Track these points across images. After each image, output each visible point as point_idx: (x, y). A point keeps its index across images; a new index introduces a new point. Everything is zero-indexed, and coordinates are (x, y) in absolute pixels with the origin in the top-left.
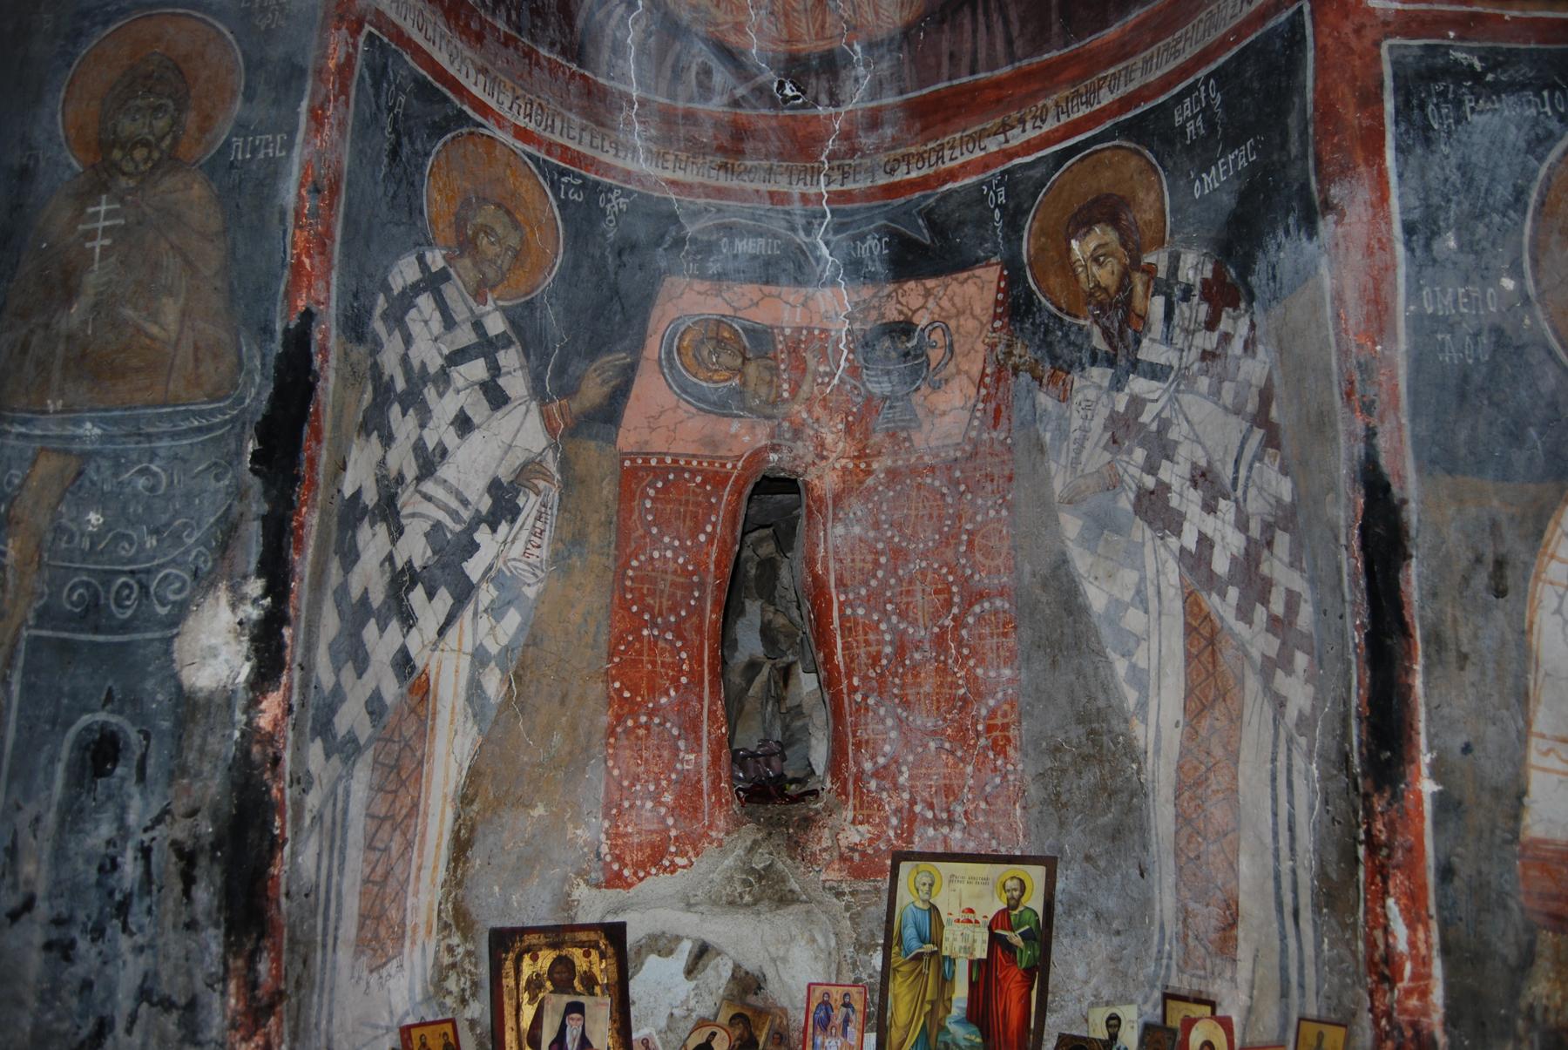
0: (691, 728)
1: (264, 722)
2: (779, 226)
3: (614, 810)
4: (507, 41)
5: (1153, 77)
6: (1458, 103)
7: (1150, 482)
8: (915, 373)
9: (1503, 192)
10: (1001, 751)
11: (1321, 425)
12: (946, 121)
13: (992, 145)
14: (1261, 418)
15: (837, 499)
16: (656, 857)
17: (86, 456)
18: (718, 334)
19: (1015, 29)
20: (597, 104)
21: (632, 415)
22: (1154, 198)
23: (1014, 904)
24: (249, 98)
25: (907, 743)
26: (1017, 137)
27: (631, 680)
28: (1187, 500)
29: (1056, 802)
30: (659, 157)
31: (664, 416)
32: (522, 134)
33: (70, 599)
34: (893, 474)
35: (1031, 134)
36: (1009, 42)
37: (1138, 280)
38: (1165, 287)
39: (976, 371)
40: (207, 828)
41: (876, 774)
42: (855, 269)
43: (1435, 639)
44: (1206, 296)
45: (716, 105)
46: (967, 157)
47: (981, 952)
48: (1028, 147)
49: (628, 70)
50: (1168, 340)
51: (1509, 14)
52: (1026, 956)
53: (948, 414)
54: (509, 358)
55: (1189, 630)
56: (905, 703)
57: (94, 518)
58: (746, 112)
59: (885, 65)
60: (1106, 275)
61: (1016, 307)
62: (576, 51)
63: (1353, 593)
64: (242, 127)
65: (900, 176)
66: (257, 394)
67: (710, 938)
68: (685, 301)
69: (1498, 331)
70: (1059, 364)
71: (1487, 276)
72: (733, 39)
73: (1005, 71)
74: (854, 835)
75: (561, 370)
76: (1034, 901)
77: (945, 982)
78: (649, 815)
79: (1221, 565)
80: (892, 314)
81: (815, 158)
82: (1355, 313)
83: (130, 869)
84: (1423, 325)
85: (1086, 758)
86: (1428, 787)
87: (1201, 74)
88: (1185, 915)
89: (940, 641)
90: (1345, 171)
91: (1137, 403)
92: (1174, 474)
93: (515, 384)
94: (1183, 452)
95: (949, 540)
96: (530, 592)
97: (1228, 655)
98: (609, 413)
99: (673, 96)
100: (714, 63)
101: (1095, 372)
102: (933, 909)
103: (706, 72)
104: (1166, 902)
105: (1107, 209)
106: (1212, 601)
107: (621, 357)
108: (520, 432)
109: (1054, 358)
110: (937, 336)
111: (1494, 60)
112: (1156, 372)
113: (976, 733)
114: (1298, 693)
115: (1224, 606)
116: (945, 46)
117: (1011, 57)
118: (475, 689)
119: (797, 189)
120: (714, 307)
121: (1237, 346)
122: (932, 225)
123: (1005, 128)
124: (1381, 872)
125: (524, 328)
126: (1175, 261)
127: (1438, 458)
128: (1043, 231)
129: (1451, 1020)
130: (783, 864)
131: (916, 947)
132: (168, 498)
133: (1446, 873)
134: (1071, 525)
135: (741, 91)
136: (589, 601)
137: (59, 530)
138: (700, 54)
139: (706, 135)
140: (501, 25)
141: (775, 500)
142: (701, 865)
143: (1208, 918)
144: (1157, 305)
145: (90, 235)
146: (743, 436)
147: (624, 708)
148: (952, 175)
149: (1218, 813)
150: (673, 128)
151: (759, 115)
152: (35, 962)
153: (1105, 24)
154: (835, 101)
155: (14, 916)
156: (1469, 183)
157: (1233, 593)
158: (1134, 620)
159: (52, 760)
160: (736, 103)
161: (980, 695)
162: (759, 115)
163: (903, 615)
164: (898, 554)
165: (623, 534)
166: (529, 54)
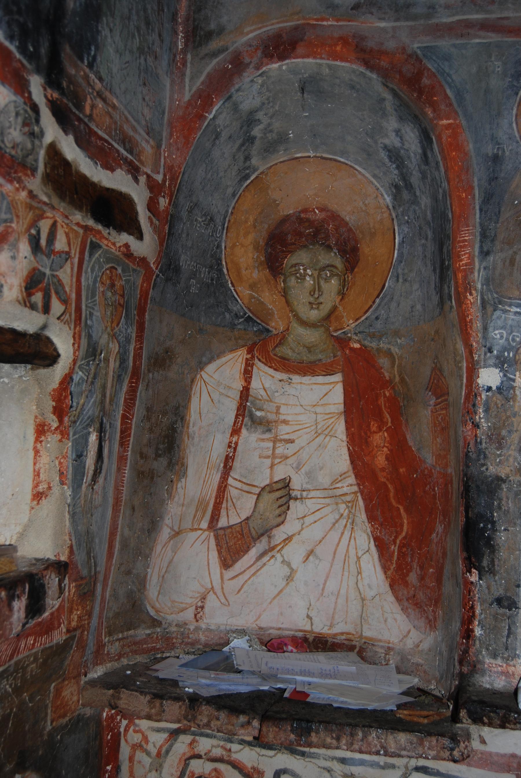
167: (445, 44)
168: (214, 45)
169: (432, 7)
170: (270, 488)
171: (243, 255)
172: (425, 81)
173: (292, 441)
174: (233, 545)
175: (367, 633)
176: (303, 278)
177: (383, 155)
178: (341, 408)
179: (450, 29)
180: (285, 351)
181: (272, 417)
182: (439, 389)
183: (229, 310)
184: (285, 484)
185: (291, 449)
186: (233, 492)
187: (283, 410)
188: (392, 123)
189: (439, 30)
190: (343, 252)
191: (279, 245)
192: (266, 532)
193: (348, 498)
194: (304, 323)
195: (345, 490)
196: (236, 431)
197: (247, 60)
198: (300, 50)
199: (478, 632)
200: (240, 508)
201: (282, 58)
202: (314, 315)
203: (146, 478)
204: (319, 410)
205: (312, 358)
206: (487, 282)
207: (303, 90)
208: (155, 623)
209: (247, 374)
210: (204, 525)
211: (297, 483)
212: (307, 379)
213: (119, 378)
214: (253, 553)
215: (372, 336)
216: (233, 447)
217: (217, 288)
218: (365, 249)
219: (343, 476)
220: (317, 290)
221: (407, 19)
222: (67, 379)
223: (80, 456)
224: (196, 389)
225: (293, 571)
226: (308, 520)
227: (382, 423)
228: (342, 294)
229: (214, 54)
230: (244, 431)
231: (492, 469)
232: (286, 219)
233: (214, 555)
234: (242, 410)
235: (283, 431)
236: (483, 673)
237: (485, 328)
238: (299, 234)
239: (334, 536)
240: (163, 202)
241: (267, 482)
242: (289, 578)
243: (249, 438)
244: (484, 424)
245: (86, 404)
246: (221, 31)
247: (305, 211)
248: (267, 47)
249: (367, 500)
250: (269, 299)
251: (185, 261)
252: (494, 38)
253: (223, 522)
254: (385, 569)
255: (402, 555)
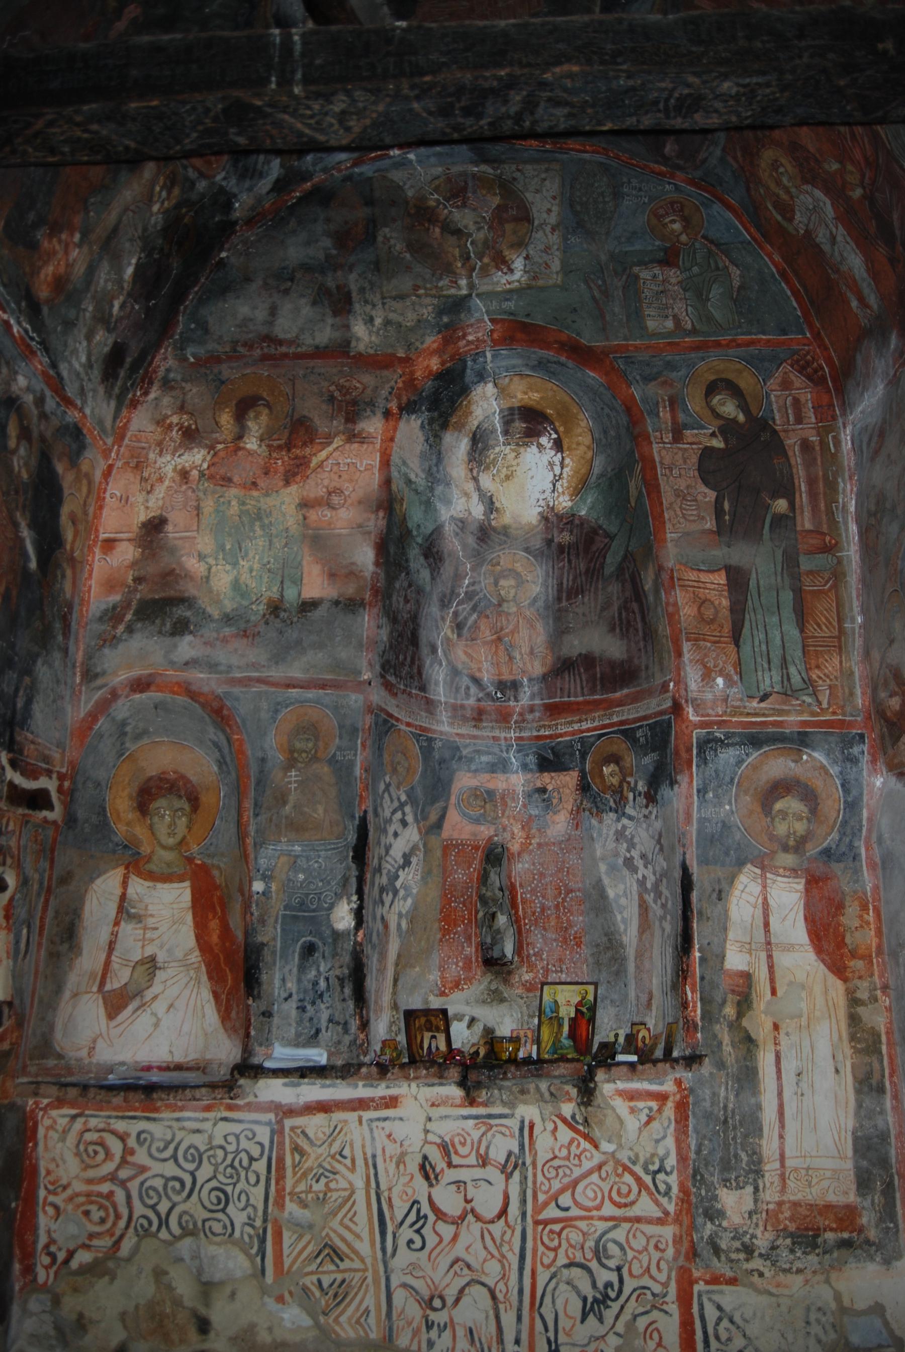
0: (468, 939)
1: (359, 939)
2: (496, 750)
3: (442, 968)
4: (404, 691)
5: (631, 717)
6: (716, 750)
7: (628, 855)
8: (548, 807)
9: (727, 779)
10: (579, 946)
11: (673, 848)
12: (559, 714)
13: (576, 727)
14: (659, 842)
15: (519, 854)
16: (457, 985)
17: (297, 857)
18: (475, 793)
19: (584, 683)
20: (430, 705)
21: (447, 825)
22: (630, 759)
23: (583, 998)
24: (341, 738)
25: (546, 944)
26: (585, 726)
27: (448, 921)
28: (639, 863)
29: (598, 963)
30: (451, 724)
31: (459, 826)
32: (408, 724)
33: (295, 902)
34: (540, 845)
35: (589, 725)
36: (582, 688)
37: (625, 785)
38: (633, 790)
39: (570, 808)
40: (346, 971)
41: (534, 955)
42: (525, 767)
43: (700, 913)
44: (645, 797)
45: (472, 701)
46: (567, 729)
47: (573, 1015)
48: (588, 730)
49: (440, 692)
50: (634, 808)
51: (734, 719)
52: (588, 1015)
53: (559, 824)
54: (408, 809)
55: (640, 906)
56: (545, 929)
57: (301, 877)
58: (483, 703)
59: (536, 688)
60: (615, 781)
61: (584, 787)
62: (423, 688)
63: (679, 899)
64: (339, 748)
65: (542, 733)
66: (352, 837)
67: (475, 1015)
68: (464, 781)
69: (723, 822)
70: (599, 810)
71: (721, 805)
72: (477, 674)
73: (581, 699)
74: (527, 977)
75: (423, 811)
76: (591, 997)
77: (560, 1026)
78: (454, 970)
79: (649, 886)
80: (539, 784)
81: (508, 722)
82: (682, 817)
83: (322, 984)
84: (701, 821)
85: (608, 948)
86: (697, 954)
87: (645, 723)
88: (638, 997)
89: (557, 907)
90: (681, 771)
91: (624, 827)
92: (635, 854)
93: (410, 818)
94: (638, 847)
95: (560, 870)
96: (415, 891)
97: (651, 915)
98: (439, 825)
99: (456, 699)
100: (471, 685)
101: (611, 814)
102: (556, 1002)
103: (468, 688)
104: (632, 994)
105: (615, 759)
106: (646, 897)
107: (441, 804)
108: (411, 835)
109: (597, 808)
110: (555, 794)
111: (728, 736)
112: (631, 818)
113: (569, 939)
114: (668, 927)
115: (649, 898)
116: (559, 685)
117: (583, 695)
118: (399, 925)
119: (503, 735)
120: (474, 782)
121: (653, 817)
122: (554, 753)
123: (580, 721)
124: (685, 978)
125: (412, 799)
126: (636, 782)
127: (704, 861)
128: (593, 762)
129: (702, 1018)
130: (502, 988)
131: (550, 1015)
132: (325, 870)
133: (702, 978)
134: (603, 868)
135: (481, 695)
136: (434, 894)
137: (289, 880)
138: (466, 681)
139: (468, 714)
140: (402, 687)
141: (494, 856)
142: (473, 988)
143: (644, 998)
144: (631, 796)
145: (290, 783)
146: (485, 831)
147: (445, 932)
148: (561, 735)
149: (647, 964)
150: (456, 710)
151: (488, 704)
152: (294, 1013)
153: (615, 691)
154: (516, 700)
155: (286, 999)
156: (717, 775)
157: (652, 895)
158: (623, 901)
159: (294, 952)
160: (479, 700)
161: (571, 926)
162: (488, 704)
163: (544, 897)
164: (542, 875)
165: (445, 870)
166: (410, 694)
167: (236, 690)
168: (99, 682)
169: (230, 667)
170: (141, 962)
171: (121, 804)
172: (225, 712)
173: (156, 929)
174: (116, 1003)
175: (208, 1057)
176: (163, 816)
177: (209, 743)
178: (189, 904)
179: (241, 682)
180: (151, 866)
181: (142, 912)
182: (241, 891)
183: (111, 841)
184: (152, 959)
185: (156, 934)
186: (115, 966)
187: (150, 907)
188: (211, 729)
189: (234, 682)
190: (189, 800)
191: (146, 797)
192: (139, 993)
193: (196, 966)
194: (164, 847)
195: (193, 960)
196: (117, 923)
197: (120, 692)
198: (153, 688)
199: (253, 1033)
200: (120, 977)
201: (141, 692)
202: (171, 841)
203: (54, 956)
204: (175, 906)
205: (170, 871)
206: (257, 831)
207: (156, 708)
208: (60, 1057)
209: (125, 884)
210: (95, 989)
211: (160, 958)
212: (166, 886)
213: (39, 895)
214: (130, 1008)
215: (209, 856)
216: (115, 934)
217: (103, 827)
218: (203, 799)
219: (191, 951)
220: (172, 825)
221: (216, 673)
222: (12, 899)
223: (17, 942)
224: (88, 896)
225: (159, 1020)
226: (169, 983)
227: (215, 913)
228: (189, 828)
229: (100, 688)
230: (123, 923)
231: (260, 939)
232: (150, 779)
233: (102, 1011)
234: (121, 909)
235: (150, 922)
236: (255, 1055)
237: (256, 858)
238: (160, 788)
239: (187, 992)
240: (67, 784)
241: (140, 958)
242: (156, 1025)
243: (127, 929)
244: (256, 914)
245: (21, 912)
246: (104, 673)
247: (163, 773)
248: (132, 685)
249: (208, 966)
250: (140, 831)
251: (81, 814)
252: (264, 688)
253: (108, 987)
254: (219, 1011)
255: (228, 1000)
